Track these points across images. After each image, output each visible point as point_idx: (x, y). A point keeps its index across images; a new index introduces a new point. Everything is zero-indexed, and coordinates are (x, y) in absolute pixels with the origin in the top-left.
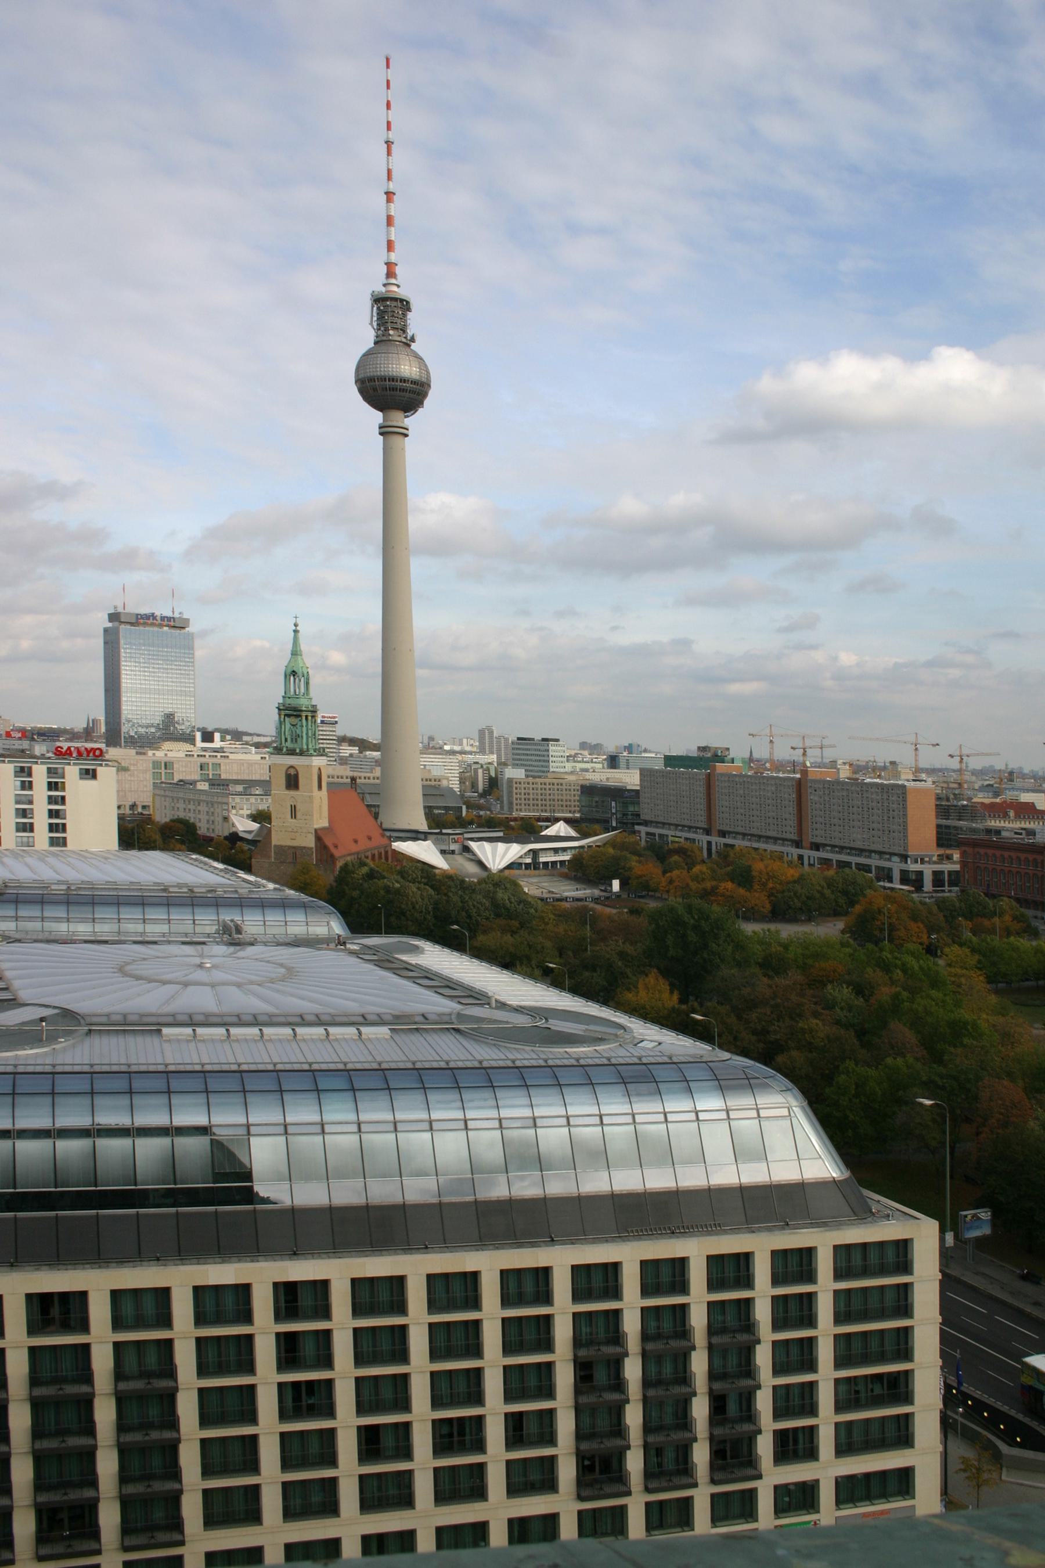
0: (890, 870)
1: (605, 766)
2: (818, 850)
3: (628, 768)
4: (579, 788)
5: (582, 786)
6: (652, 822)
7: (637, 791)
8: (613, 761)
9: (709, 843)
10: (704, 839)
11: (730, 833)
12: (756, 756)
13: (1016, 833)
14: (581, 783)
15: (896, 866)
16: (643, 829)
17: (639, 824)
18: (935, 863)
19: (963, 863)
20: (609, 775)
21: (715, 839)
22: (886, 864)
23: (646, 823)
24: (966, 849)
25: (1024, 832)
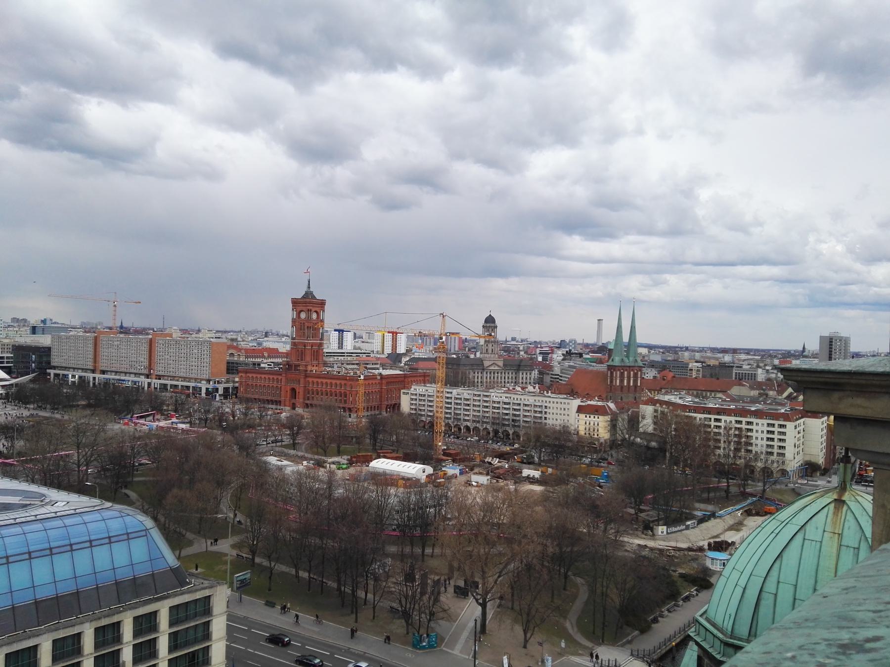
0: (200, 388)
1: (28, 333)
2: (160, 379)
3: (43, 334)
4: (11, 347)
5: (13, 346)
6: (58, 367)
7: (49, 349)
8: (34, 330)
9: (149, 384)
10: (91, 376)
11: (108, 371)
12: (124, 325)
13: (268, 365)
14: (12, 344)
15: (204, 386)
16: (52, 372)
17: (49, 369)
18: (225, 383)
19: (241, 383)
20: (32, 339)
21: (97, 376)
22: (199, 385)
23: (54, 368)
24: (243, 374)
25: (272, 364)
